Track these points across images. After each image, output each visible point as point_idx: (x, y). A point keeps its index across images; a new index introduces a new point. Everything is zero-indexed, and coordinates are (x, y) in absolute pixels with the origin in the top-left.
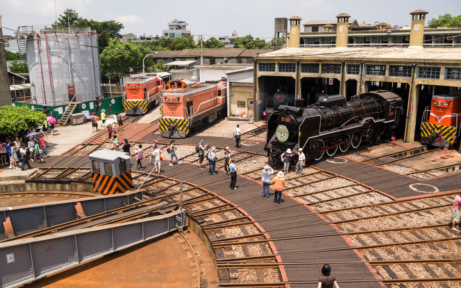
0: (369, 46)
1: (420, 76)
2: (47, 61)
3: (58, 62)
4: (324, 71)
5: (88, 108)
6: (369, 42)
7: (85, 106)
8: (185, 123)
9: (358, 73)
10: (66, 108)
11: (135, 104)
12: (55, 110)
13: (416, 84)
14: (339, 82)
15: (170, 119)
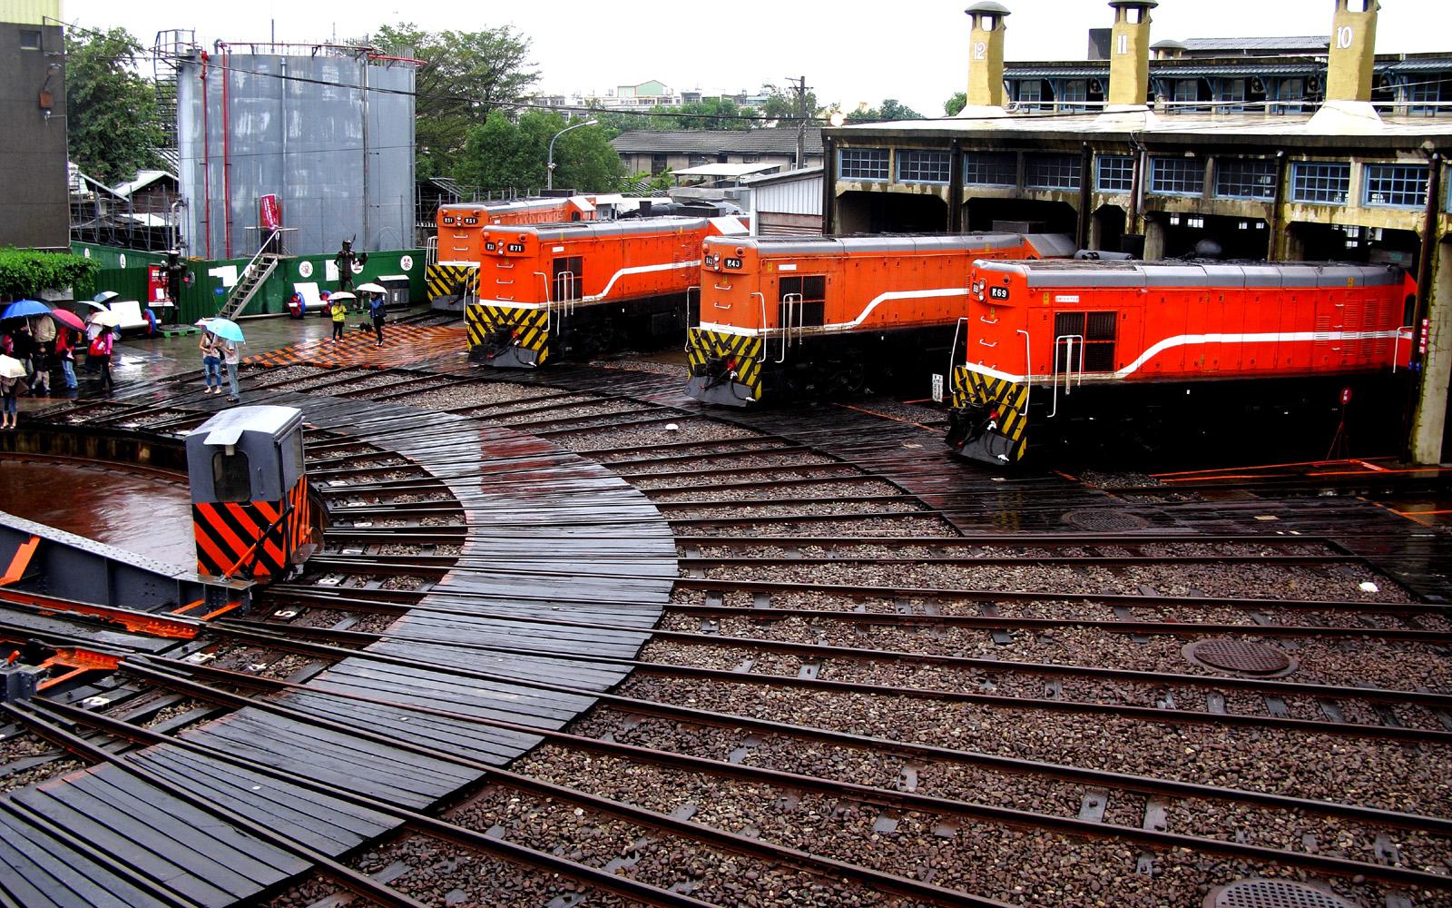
0: (1262, 108)
1: (1299, 195)
2: (222, 132)
3: (251, 134)
4: (1033, 179)
5: (318, 276)
6: (1262, 98)
7: (311, 272)
8: (540, 323)
9: (1127, 186)
10: (247, 272)
11: (462, 275)
12: (212, 272)
13: (1287, 221)
14: (1074, 213)
15: (498, 309)
